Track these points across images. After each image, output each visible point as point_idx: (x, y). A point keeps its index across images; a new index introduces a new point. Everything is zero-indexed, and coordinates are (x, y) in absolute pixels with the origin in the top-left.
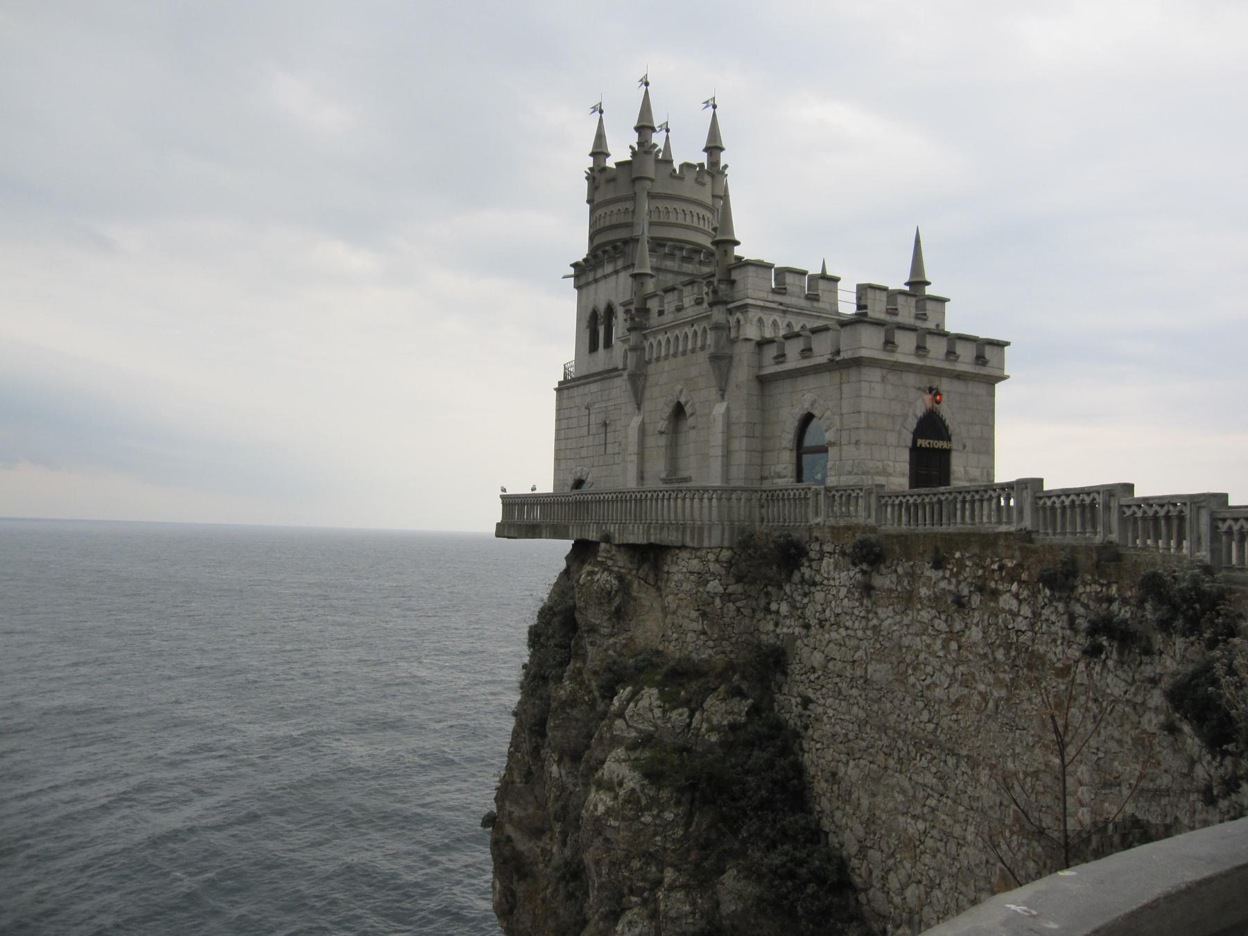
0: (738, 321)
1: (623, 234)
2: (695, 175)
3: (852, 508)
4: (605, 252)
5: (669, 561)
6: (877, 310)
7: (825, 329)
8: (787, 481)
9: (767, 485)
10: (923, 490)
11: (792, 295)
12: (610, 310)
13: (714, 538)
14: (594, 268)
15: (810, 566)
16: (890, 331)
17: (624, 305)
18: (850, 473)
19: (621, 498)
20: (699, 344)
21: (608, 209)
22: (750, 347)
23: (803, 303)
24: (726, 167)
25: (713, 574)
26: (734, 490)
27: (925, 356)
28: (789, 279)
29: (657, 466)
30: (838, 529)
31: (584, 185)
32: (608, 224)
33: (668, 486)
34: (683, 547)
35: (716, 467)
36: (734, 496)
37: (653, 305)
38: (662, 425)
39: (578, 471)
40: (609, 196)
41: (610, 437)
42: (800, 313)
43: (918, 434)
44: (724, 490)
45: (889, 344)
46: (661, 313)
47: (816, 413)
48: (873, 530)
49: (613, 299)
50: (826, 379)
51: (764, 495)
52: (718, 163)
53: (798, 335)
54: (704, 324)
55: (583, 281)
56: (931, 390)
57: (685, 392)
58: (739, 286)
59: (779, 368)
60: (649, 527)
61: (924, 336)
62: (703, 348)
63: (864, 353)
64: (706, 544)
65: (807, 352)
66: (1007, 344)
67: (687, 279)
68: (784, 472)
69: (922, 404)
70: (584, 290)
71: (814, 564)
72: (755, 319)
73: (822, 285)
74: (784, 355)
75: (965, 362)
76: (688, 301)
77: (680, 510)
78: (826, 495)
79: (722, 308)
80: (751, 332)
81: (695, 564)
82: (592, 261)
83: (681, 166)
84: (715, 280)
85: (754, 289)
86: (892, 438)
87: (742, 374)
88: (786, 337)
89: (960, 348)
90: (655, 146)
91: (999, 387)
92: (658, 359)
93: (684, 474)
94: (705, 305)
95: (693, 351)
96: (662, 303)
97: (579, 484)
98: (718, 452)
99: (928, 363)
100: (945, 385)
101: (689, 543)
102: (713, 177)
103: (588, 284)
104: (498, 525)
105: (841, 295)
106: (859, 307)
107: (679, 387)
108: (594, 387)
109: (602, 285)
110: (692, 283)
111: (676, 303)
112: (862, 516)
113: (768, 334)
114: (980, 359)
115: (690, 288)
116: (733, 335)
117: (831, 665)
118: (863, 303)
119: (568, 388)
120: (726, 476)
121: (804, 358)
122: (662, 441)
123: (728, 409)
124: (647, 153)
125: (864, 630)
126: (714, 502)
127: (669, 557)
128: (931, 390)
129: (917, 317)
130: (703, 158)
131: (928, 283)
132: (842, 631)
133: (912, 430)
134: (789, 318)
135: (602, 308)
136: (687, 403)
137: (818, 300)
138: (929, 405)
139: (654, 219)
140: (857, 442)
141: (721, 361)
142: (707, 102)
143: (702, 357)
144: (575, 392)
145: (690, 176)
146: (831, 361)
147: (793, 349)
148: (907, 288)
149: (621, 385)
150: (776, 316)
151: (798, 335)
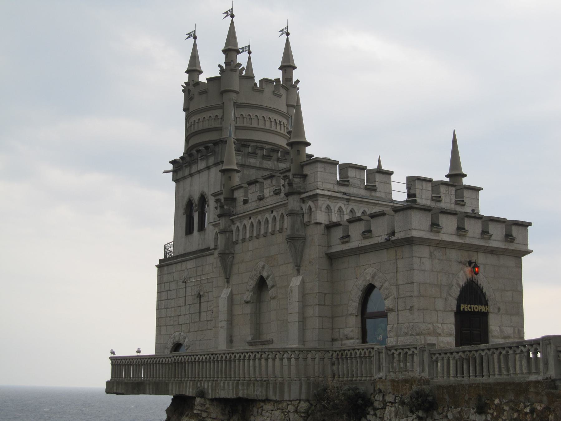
0: (310, 208)
1: (214, 136)
2: (272, 89)
3: (408, 364)
4: (198, 151)
5: (255, 413)
6: (424, 198)
7: (383, 214)
8: (354, 342)
9: (337, 346)
10: (467, 348)
11: (354, 186)
12: (203, 200)
13: (294, 392)
14: (190, 165)
15: (375, 415)
16: (435, 215)
17: (214, 195)
18: (406, 334)
19: (213, 359)
20: (278, 227)
21: (201, 116)
22: (321, 229)
23: (363, 192)
24: (298, 81)
26: (309, 351)
27: (464, 236)
28: (351, 173)
29: (244, 332)
30: (398, 382)
31: (181, 96)
32: (201, 128)
33: (253, 348)
34: (267, 400)
35: (294, 330)
36: (309, 356)
37: (239, 195)
38: (248, 296)
39: (177, 336)
40: (202, 106)
41: (204, 306)
42: (361, 201)
43: (461, 299)
44: (300, 351)
45: (435, 226)
46: (246, 202)
47: (377, 284)
48: (427, 382)
49: (206, 190)
50: (384, 255)
51: (335, 355)
52: (291, 79)
53: (359, 219)
54: (282, 211)
55: (180, 175)
56: (470, 263)
57: (266, 267)
58: (310, 179)
59: (345, 247)
60: (237, 385)
61: (463, 220)
62: (281, 231)
63: (415, 234)
64: (286, 397)
65: (367, 233)
66: (530, 224)
67: (267, 173)
68: (352, 335)
69: (463, 276)
70: (181, 183)
71: (378, 413)
72: (324, 206)
73: (378, 177)
74: (348, 236)
75: (497, 240)
76: (268, 192)
77: (263, 369)
78: (387, 354)
79: (296, 197)
80: (321, 217)
82: (188, 159)
83: (261, 81)
84: (290, 174)
85: (323, 182)
86: (440, 304)
87: (314, 252)
88: (350, 221)
89: (493, 229)
90: (240, 65)
91: (525, 259)
92: (243, 240)
93: (268, 337)
94: (282, 195)
95: (273, 233)
96: (246, 194)
97: (177, 347)
98: (295, 318)
99: (467, 241)
100: (481, 259)
101: (271, 396)
102: (287, 89)
103: (184, 178)
104: (108, 383)
105: (394, 186)
106: (409, 195)
107: (261, 264)
108: (190, 264)
109: (196, 178)
110: (271, 177)
111: (258, 194)
112: (417, 370)
113: (335, 218)
114: (509, 237)
115: (269, 181)
116: (306, 219)
118: (412, 192)
119: (168, 265)
120: (302, 340)
121: (365, 238)
122: (248, 309)
123: (303, 282)
124: (235, 70)
126: (293, 360)
127: (255, 409)
128: (470, 263)
129: (457, 203)
130: (279, 75)
131: (465, 176)
133: (456, 297)
134: (352, 205)
135: (196, 198)
136: (268, 277)
137: (375, 190)
138: (469, 276)
139: (238, 125)
140: (411, 308)
141: (296, 241)
142: (282, 31)
143: (280, 238)
144: (174, 268)
145: (268, 90)
146: (388, 240)
147: (356, 231)
148: (448, 180)
149: (212, 262)
150: (341, 204)
151: (359, 219)
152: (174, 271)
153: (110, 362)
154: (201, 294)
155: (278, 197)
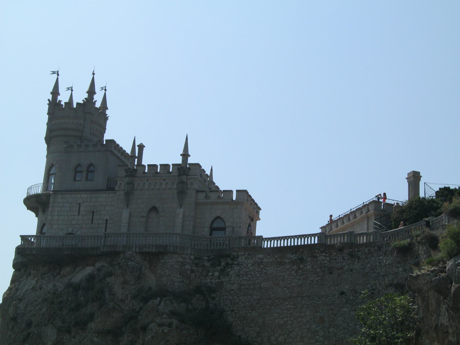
25: (187, 263)
59: (208, 201)
64: (185, 253)
81: (180, 259)
92: (141, 190)
101: (179, 252)
108: (83, 196)
116: (189, 186)
117: (242, 287)
123: (184, 211)
125: (260, 274)
132: (250, 276)
152: (69, 197)
153: (20, 238)
154: (95, 211)
155: (169, 175)
